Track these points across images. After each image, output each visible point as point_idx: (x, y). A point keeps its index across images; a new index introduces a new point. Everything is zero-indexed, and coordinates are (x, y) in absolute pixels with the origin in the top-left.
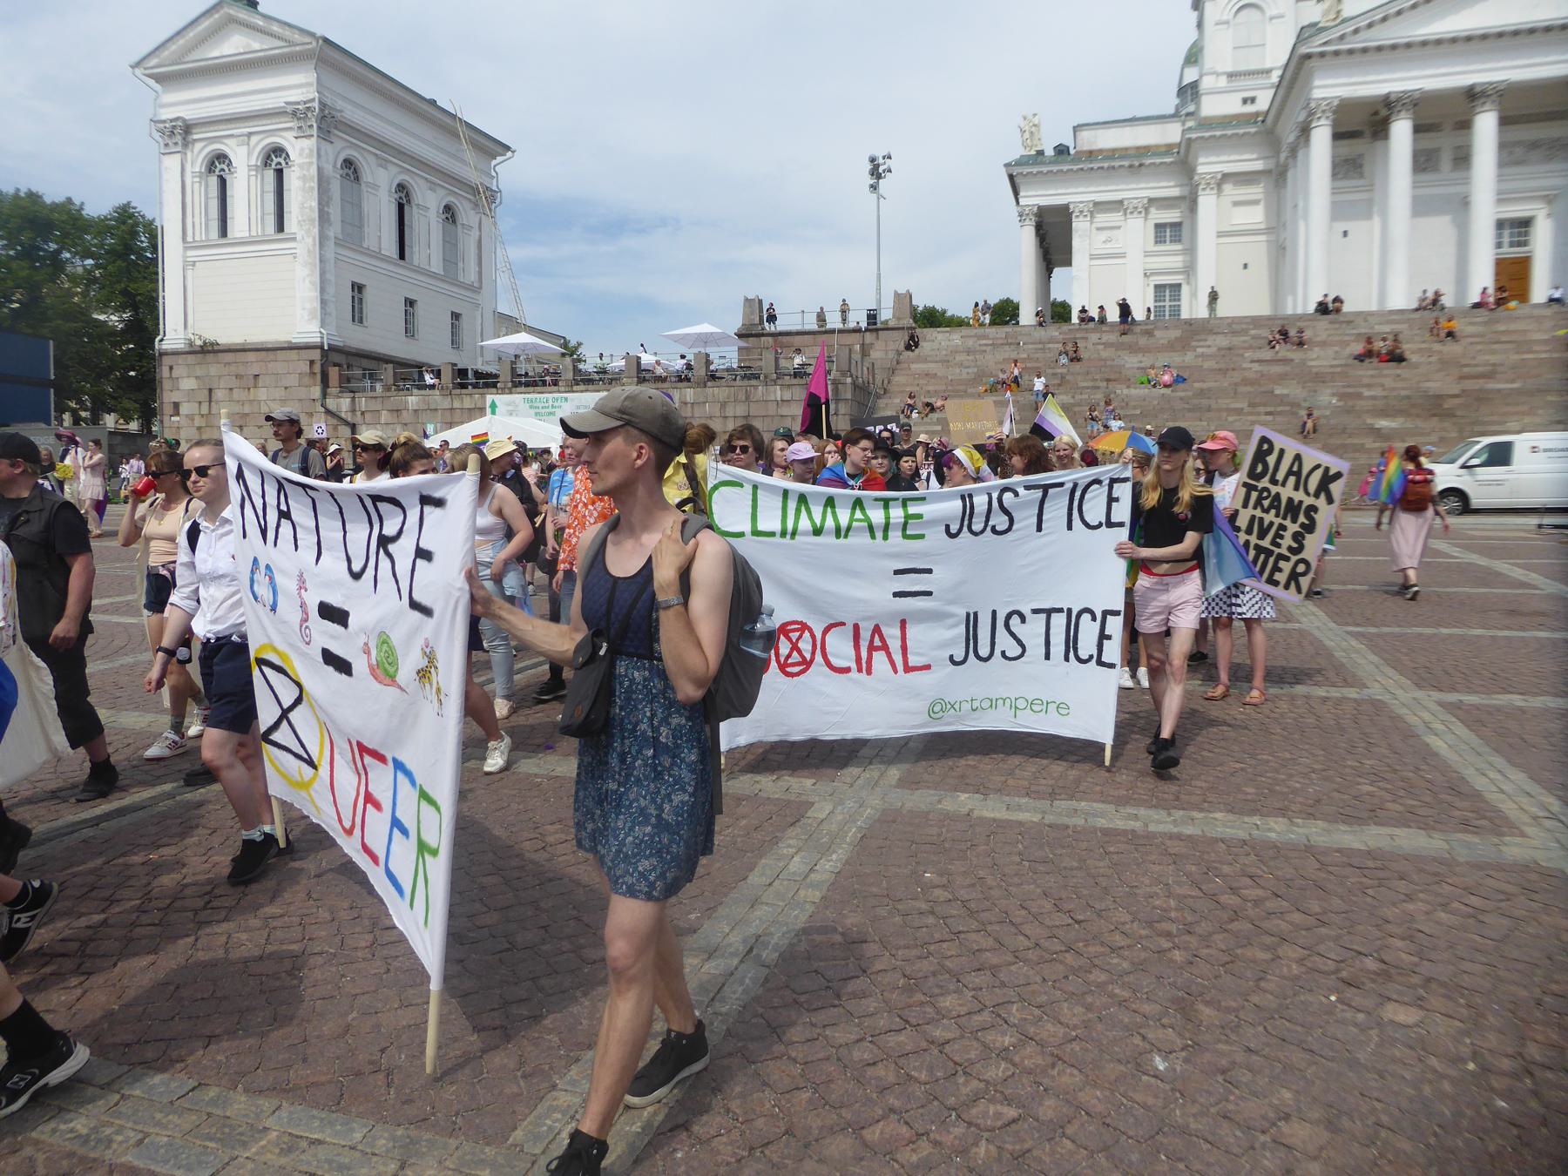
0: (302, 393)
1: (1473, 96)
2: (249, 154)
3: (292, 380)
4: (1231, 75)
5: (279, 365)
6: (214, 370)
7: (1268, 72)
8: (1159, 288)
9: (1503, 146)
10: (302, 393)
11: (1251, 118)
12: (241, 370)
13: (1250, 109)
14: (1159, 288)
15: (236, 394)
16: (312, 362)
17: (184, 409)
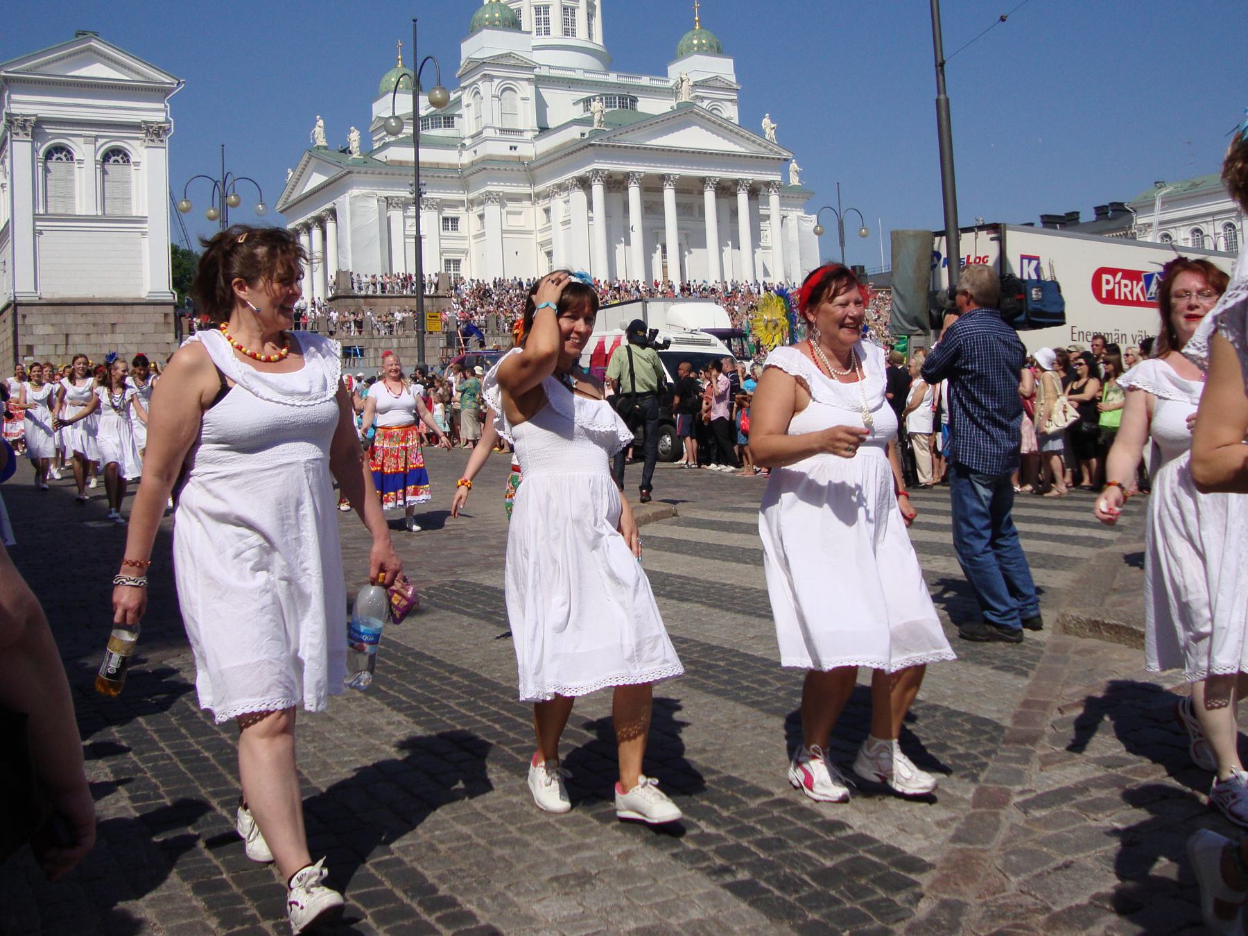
0: (158, 338)
1: (663, 178)
2: (96, 153)
3: (150, 328)
4: (501, 130)
5: (135, 316)
6: (70, 319)
7: (521, 132)
8: (448, 262)
9: (678, 205)
10: (158, 338)
11: (519, 160)
12: (99, 319)
13: (513, 153)
14: (448, 262)
15: (93, 338)
16: (166, 315)
17: (38, 351)
